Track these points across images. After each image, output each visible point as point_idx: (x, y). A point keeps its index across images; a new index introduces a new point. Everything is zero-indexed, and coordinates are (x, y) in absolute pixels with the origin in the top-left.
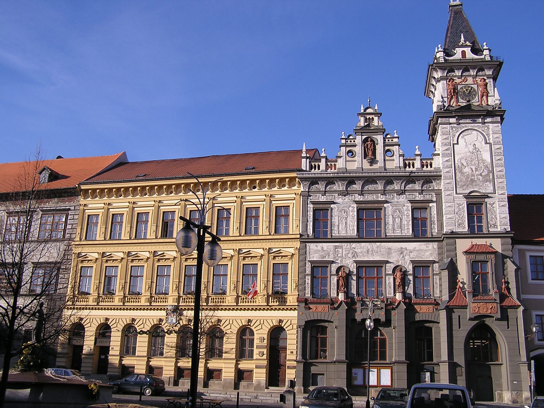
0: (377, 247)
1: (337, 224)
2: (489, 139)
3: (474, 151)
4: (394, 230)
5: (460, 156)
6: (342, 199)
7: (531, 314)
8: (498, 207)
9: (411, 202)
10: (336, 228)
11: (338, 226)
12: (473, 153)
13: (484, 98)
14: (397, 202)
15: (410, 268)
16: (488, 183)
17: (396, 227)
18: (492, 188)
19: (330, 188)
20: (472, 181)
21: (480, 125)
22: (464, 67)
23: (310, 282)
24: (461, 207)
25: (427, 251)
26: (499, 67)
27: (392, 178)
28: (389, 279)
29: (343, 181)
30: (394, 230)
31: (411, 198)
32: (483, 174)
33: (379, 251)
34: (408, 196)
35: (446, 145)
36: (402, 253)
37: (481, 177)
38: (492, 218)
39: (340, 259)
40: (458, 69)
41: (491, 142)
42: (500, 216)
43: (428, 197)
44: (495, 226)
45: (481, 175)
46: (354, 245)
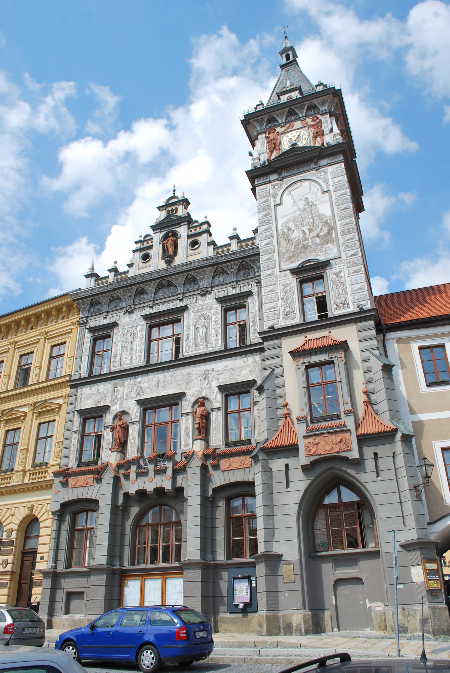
0: (172, 376)
1: (119, 352)
2: (328, 186)
3: (307, 206)
4: (196, 345)
5: (285, 219)
6: (129, 318)
7: (431, 448)
8: (347, 275)
9: (220, 300)
10: (118, 359)
11: (121, 355)
12: (304, 210)
13: (318, 138)
14: (202, 305)
15: (217, 400)
16: (330, 245)
17: (199, 340)
18: (336, 250)
19: (115, 306)
20: (305, 247)
21: (314, 172)
22: (287, 110)
23: (76, 443)
24: (288, 288)
25: (244, 369)
26: (336, 99)
27: (192, 273)
28: (187, 421)
29: (129, 291)
30: (196, 345)
31: (221, 295)
32: (321, 234)
33: (173, 381)
34: (217, 294)
35: (264, 209)
36: (206, 378)
37: (318, 240)
38: (339, 294)
39: (119, 402)
40: (281, 115)
41: (331, 188)
42: (351, 288)
43: (246, 289)
44: (345, 304)
45: (318, 236)
46: (139, 379)
